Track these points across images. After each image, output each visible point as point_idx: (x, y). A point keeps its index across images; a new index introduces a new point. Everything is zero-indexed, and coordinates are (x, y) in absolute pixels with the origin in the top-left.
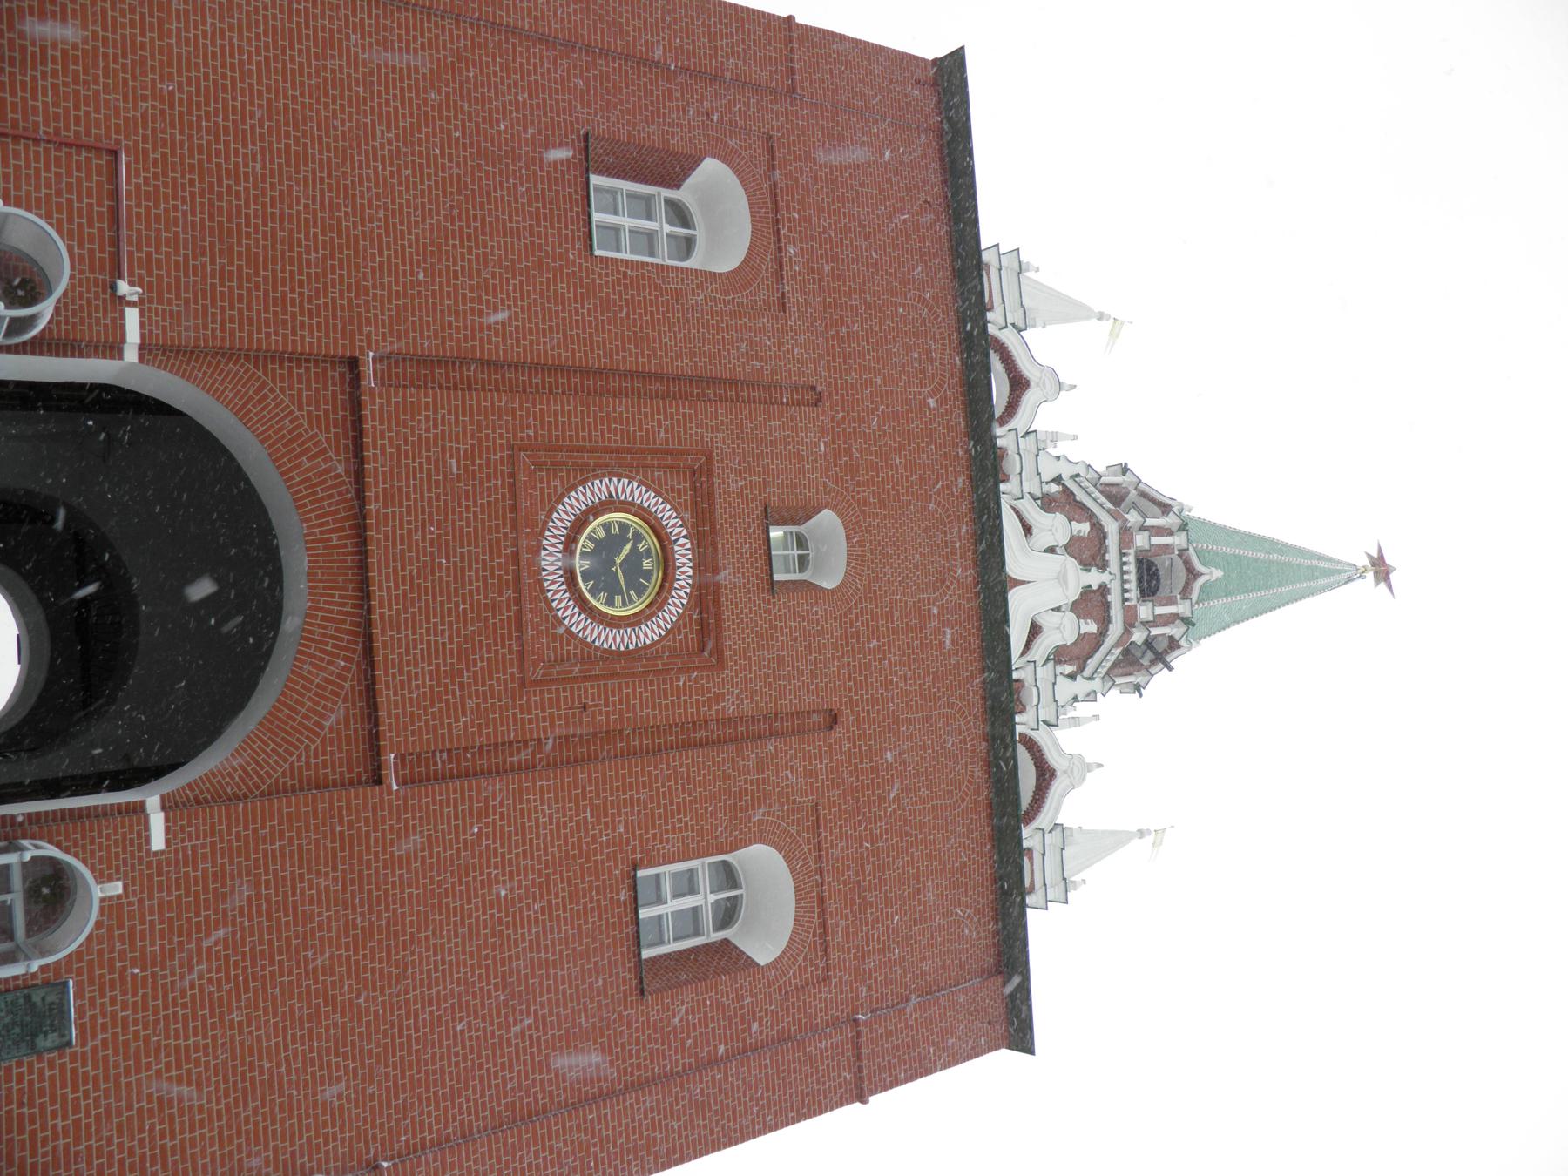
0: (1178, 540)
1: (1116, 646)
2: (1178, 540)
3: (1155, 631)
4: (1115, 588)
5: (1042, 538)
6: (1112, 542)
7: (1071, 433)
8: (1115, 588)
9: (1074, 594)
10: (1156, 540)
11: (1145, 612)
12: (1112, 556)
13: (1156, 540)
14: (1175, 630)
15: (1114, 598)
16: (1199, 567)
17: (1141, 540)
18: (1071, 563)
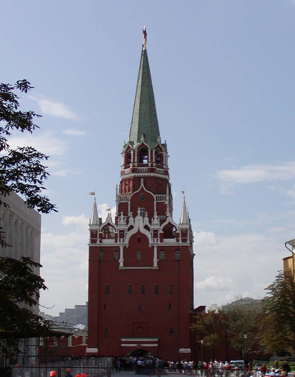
0: (136, 152)
1: (155, 172)
2: (136, 152)
3: (154, 161)
4: (144, 174)
5: (133, 224)
6: (136, 174)
7: (116, 185)
8: (144, 174)
9: (141, 218)
10: (136, 161)
11: (150, 165)
12: (139, 174)
13: (136, 161)
14: (154, 151)
15: (146, 174)
16: (142, 142)
17: (136, 165)
18: (137, 218)
